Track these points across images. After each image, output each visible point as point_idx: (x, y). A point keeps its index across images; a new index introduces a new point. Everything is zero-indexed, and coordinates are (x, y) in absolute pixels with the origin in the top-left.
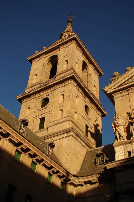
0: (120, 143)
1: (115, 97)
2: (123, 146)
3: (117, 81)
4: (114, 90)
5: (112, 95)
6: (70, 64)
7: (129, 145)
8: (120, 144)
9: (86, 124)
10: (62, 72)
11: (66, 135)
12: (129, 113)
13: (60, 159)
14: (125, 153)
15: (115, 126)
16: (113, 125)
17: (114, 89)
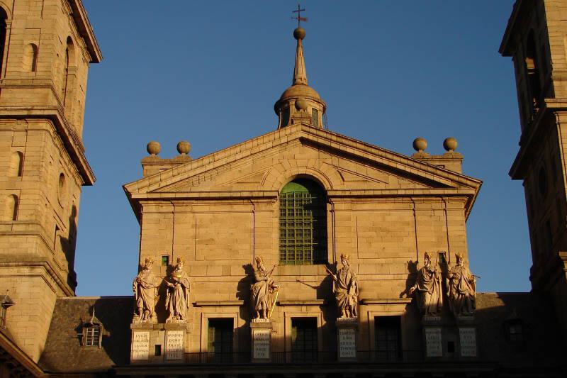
0: (144, 324)
1: (145, 209)
2: (148, 333)
3: (158, 179)
4: (145, 196)
5: (141, 202)
6: (46, 64)
7: (160, 332)
8: (145, 327)
9: (57, 226)
10: (19, 83)
11: (26, 271)
12: (168, 257)
13: (10, 323)
14: (150, 346)
15: (139, 285)
16: (136, 285)
17: (147, 193)
